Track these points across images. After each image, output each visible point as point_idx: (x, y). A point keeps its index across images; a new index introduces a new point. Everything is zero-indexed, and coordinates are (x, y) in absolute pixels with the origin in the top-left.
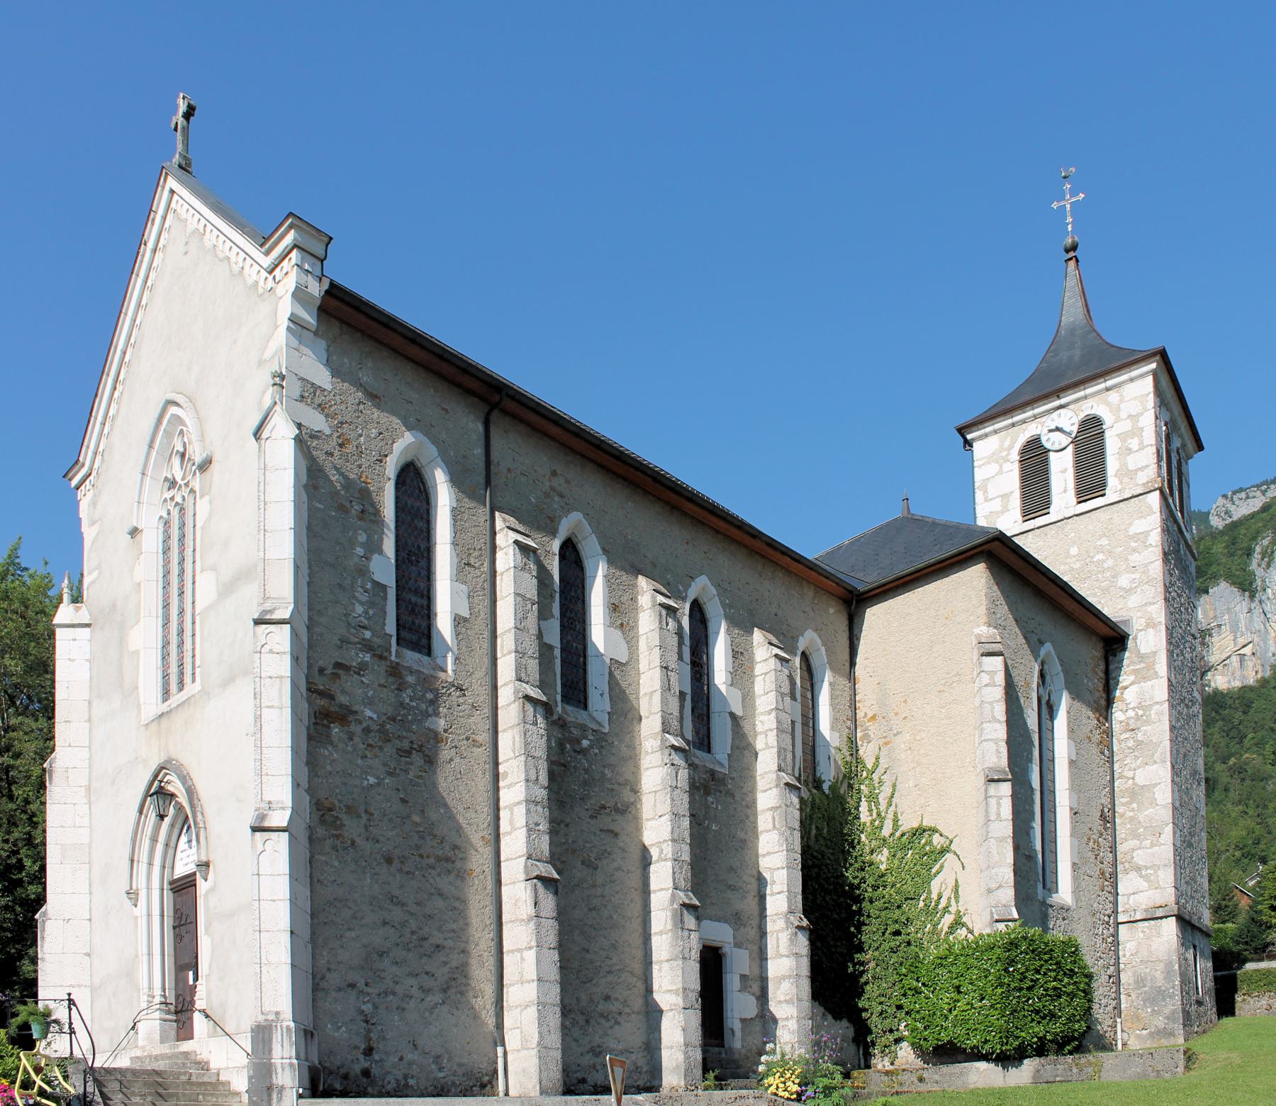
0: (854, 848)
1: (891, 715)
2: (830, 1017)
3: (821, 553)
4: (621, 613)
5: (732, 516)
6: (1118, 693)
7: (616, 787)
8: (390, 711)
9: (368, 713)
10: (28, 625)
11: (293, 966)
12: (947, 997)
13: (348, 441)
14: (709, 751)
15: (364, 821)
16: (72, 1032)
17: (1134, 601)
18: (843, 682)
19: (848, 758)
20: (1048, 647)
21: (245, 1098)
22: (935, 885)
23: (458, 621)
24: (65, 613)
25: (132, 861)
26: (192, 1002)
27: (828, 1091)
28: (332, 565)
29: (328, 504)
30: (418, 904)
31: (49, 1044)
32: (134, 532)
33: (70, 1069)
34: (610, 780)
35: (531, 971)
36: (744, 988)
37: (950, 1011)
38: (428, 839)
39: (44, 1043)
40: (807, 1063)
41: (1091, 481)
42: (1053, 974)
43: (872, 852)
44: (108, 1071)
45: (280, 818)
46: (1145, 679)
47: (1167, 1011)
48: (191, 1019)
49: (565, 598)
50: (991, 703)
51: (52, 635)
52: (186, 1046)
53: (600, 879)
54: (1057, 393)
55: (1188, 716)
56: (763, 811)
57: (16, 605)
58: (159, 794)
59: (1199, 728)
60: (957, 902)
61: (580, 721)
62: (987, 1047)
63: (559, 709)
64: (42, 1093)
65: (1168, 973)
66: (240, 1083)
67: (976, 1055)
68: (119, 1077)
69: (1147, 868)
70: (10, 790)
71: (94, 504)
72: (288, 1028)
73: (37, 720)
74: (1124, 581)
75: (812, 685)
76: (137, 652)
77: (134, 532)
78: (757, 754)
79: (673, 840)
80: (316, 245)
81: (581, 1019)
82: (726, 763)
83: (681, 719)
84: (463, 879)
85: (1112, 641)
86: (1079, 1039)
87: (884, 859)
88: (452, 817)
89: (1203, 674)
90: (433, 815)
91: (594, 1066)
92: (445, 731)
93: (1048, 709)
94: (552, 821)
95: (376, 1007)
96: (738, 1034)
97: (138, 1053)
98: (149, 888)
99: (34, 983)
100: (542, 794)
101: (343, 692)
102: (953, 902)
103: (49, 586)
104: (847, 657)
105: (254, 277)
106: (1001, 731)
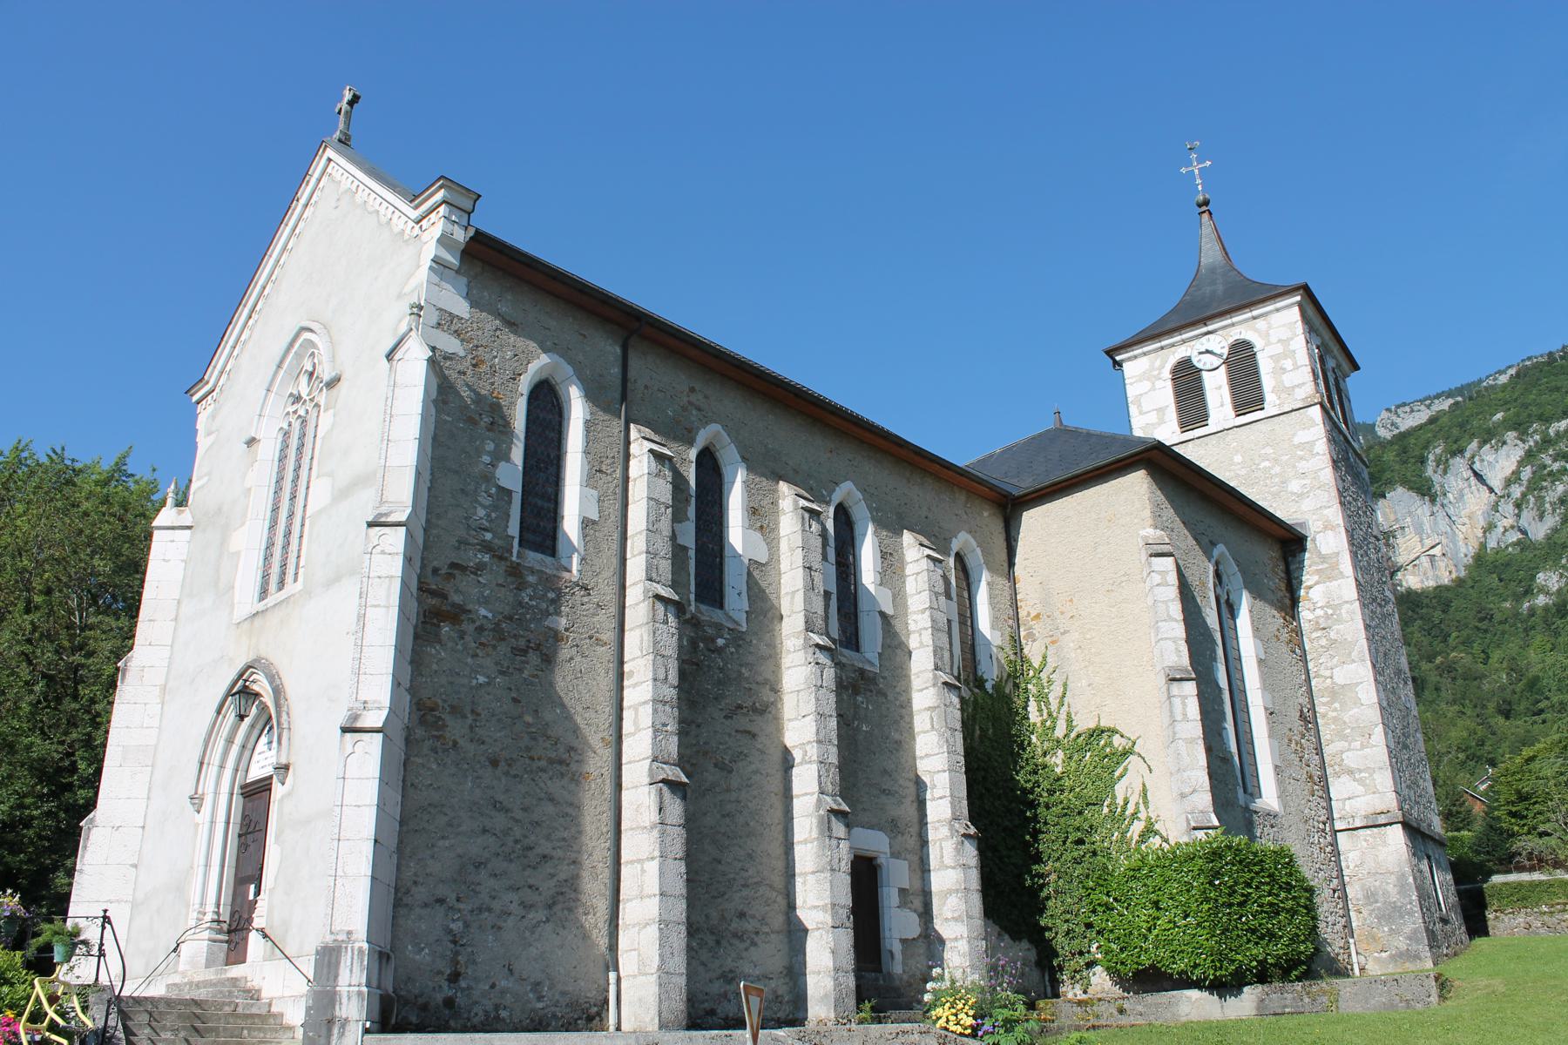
0: (1024, 750)
1: (1057, 614)
2: (1006, 937)
3: (973, 459)
4: (761, 518)
5: (877, 427)
6: (1302, 592)
7: (754, 686)
8: (507, 610)
9: (483, 612)
10: (125, 527)
11: (373, 878)
12: (1145, 913)
13: (483, 362)
14: (858, 650)
15: (469, 721)
16: (102, 954)
17: (1307, 505)
18: (1002, 582)
19: (1012, 657)
20: (1220, 549)
21: (300, 1033)
22: (1120, 790)
23: (586, 524)
24: (166, 516)
25: (202, 764)
26: (250, 920)
27: (1009, 1025)
28: (456, 472)
29: (457, 420)
30: (525, 810)
31: (72, 968)
32: (251, 442)
33: (91, 999)
34: (747, 679)
35: (652, 883)
36: (903, 904)
37: (1149, 930)
38: (541, 740)
39: (66, 967)
40: (983, 991)
41: (1247, 395)
42: (1267, 888)
43: (1045, 754)
44: (138, 1001)
45: (376, 718)
46: (1330, 579)
47: (1407, 930)
48: (246, 939)
49: (702, 504)
50: (1165, 602)
51: (149, 536)
52: (236, 971)
53: (735, 783)
54: (1204, 321)
55: (1383, 615)
56: (920, 711)
57: (115, 509)
58: (242, 693)
59: (1396, 627)
60: (1147, 808)
61: (715, 619)
62: (1198, 972)
63: (693, 608)
64: (53, 1027)
65: (1402, 887)
66: (295, 1015)
67: (1184, 982)
68: (149, 1007)
69: (1360, 771)
70: (76, 689)
71: (213, 417)
72: (361, 950)
73: (118, 619)
74: (1294, 486)
75: (969, 585)
76: (238, 554)
77: (251, 442)
78: (910, 653)
79: (819, 742)
80: (464, 201)
81: (710, 939)
82: (877, 663)
83: (826, 618)
84: (578, 783)
85: (1289, 543)
86: (1308, 963)
87: (1059, 761)
88: (569, 717)
89: (1392, 574)
90: (548, 716)
91: (725, 995)
92: (567, 630)
93: (1228, 609)
94: (682, 721)
95: (467, 925)
96: (898, 956)
97: (177, 979)
98: (216, 793)
99: (66, 898)
100: (670, 693)
101: (457, 591)
102: (1142, 807)
103: (154, 490)
104: (1004, 556)
105: (401, 226)
106: (1179, 630)
